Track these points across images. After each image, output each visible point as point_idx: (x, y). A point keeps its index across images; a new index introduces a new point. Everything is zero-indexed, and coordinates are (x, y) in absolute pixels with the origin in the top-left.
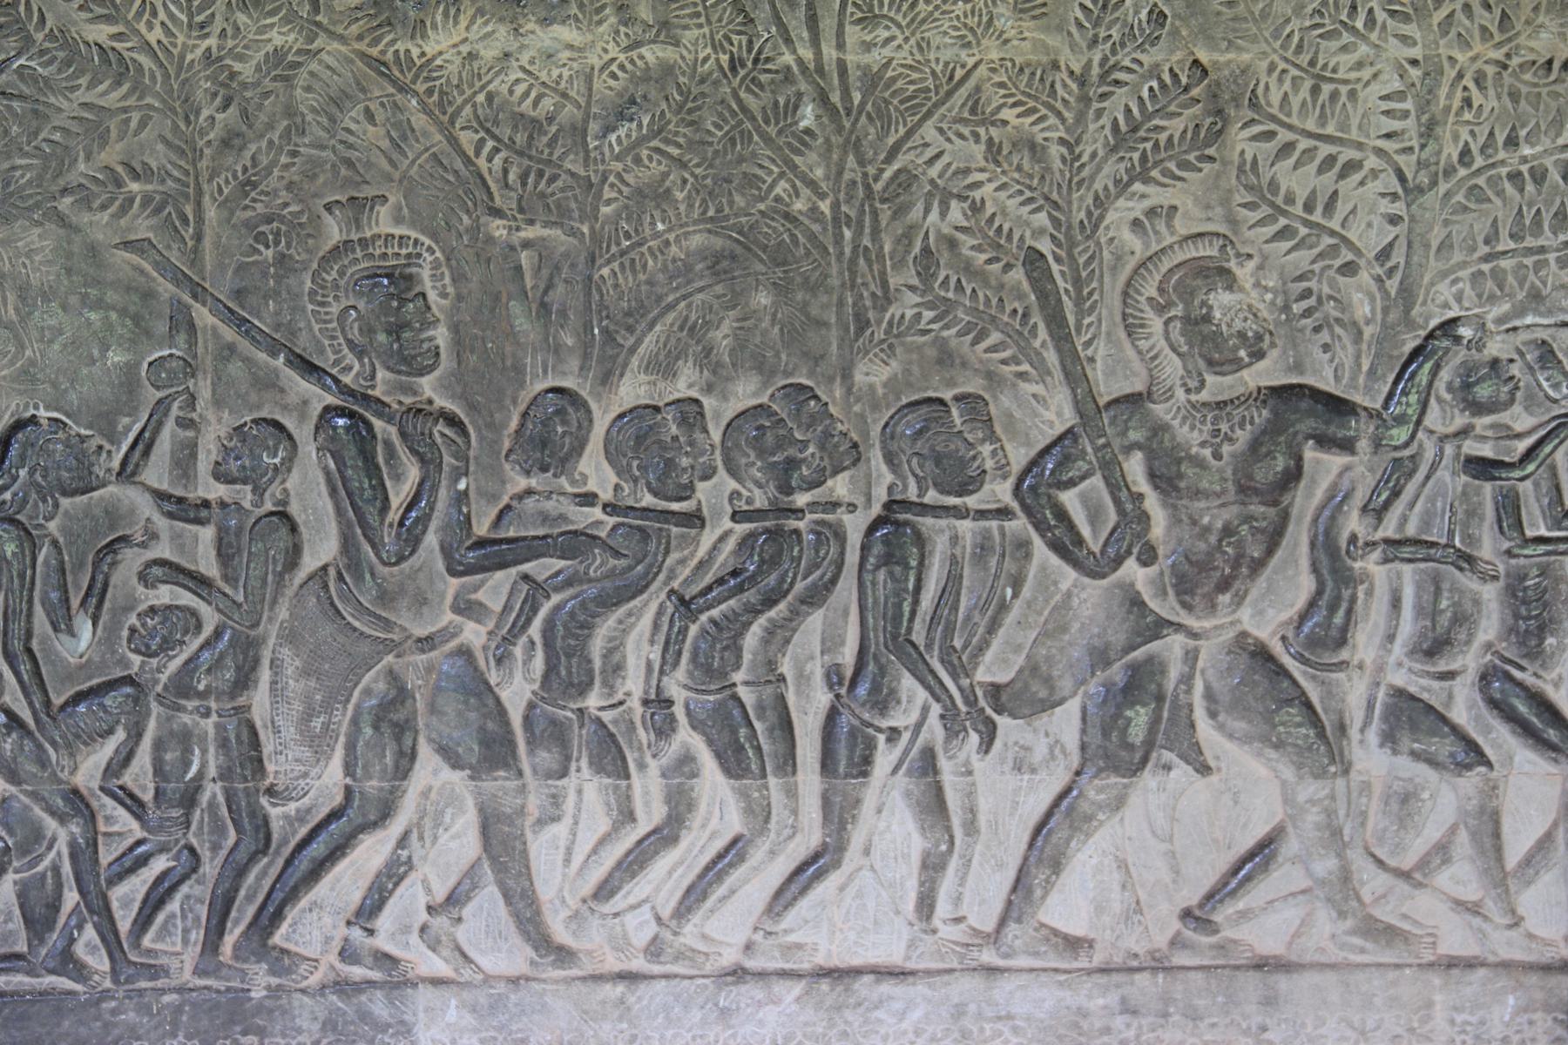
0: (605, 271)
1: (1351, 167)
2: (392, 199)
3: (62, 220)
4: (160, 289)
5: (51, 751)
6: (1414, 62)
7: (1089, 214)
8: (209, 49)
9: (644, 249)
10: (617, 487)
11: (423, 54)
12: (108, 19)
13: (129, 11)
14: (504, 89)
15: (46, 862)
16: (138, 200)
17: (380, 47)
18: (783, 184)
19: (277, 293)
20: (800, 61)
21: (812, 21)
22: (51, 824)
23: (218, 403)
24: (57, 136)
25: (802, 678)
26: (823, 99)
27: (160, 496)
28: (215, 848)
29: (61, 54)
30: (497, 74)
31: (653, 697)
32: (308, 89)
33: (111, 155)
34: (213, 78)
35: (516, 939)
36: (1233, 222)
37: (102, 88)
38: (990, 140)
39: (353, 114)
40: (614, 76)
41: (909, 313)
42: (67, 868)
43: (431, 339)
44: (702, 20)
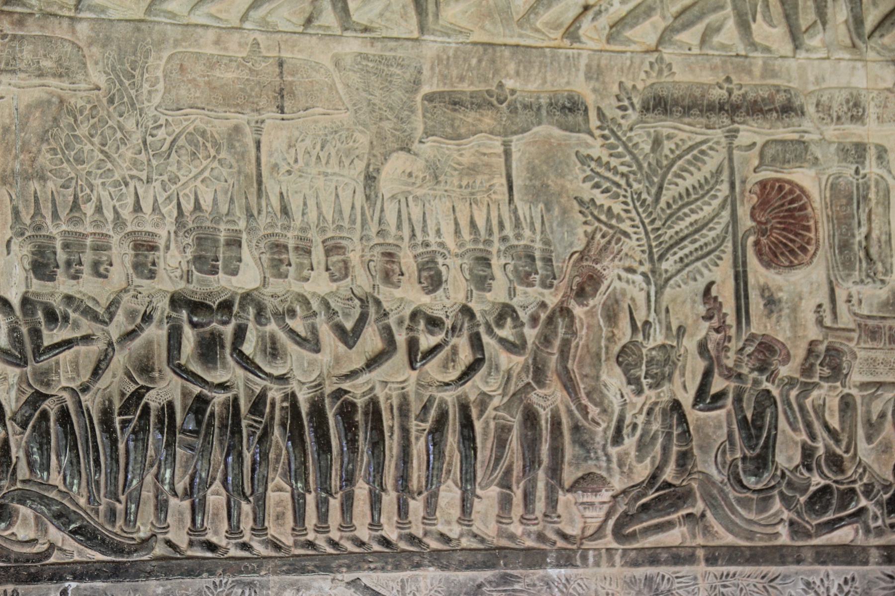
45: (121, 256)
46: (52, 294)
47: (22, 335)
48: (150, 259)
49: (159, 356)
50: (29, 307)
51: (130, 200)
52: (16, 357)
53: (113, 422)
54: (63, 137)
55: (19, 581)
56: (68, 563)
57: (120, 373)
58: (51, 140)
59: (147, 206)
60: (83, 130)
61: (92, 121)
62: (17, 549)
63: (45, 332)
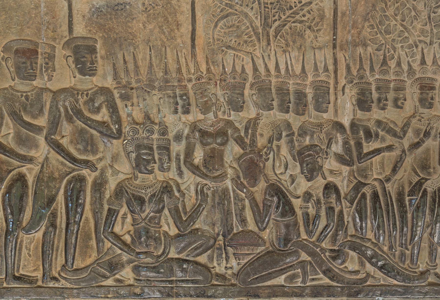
45: (412, 94)
46: (369, 120)
47: (351, 146)
48: (430, 95)
49: (434, 158)
50: (355, 128)
51: (418, 57)
52: (348, 160)
53: (404, 201)
54: (378, 17)
56: (378, 286)
57: (409, 169)
58: (371, 19)
59: (429, 61)
60: (390, 12)
61: (396, 5)
62: (348, 276)
63: (364, 144)
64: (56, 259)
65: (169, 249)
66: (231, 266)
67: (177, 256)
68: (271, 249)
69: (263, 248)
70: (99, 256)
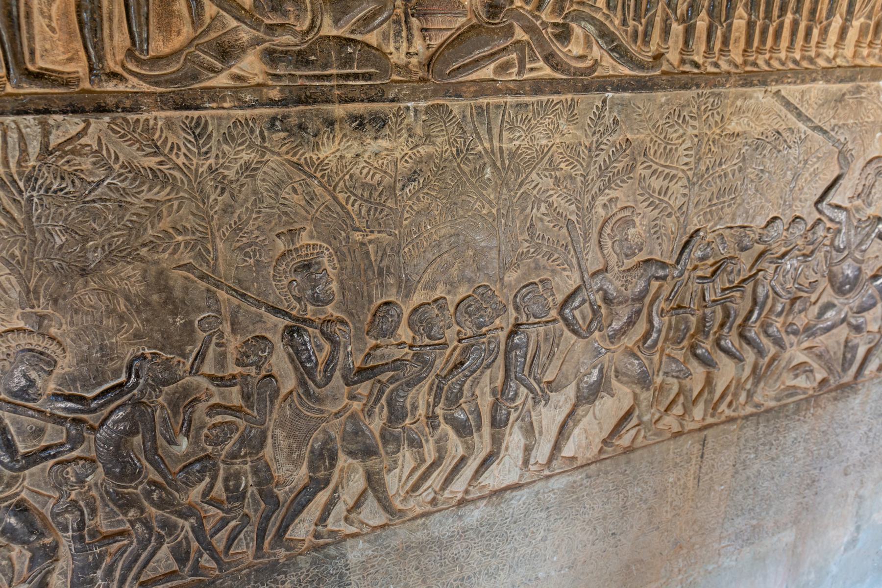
0: (406, 250)
1: (674, 176)
2: (308, 228)
3: (142, 259)
4: (200, 286)
5: (176, 493)
6: (696, 136)
7: (590, 203)
8: (210, 166)
9: (422, 238)
10: (414, 338)
11: (319, 158)
12: (155, 154)
13: (164, 149)
14: (358, 171)
15: (181, 536)
16: (183, 244)
17: (298, 156)
18: (478, 203)
19: (257, 279)
20: (484, 148)
21: (489, 131)
22: (181, 522)
23: (234, 331)
24: (134, 218)
25: (483, 394)
26: (494, 165)
27: (212, 378)
28: (256, 511)
29: (131, 175)
30: (355, 164)
31: (430, 415)
32: (264, 180)
33: (165, 224)
34: (215, 179)
35: (382, 512)
36: (636, 201)
37: (155, 190)
38: (556, 177)
39: (287, 190)
40: (407, 161)
41: (525, 250)
42: (191, 535)
43: (330, 289)
44: (445, 133)
55: (576, 91)
64: (111, 37)
65: (322, 20)
66: (415, 51)
67: (334, 33)
68: (474, 21)
69: (464, 19)
70: (196, 31)
